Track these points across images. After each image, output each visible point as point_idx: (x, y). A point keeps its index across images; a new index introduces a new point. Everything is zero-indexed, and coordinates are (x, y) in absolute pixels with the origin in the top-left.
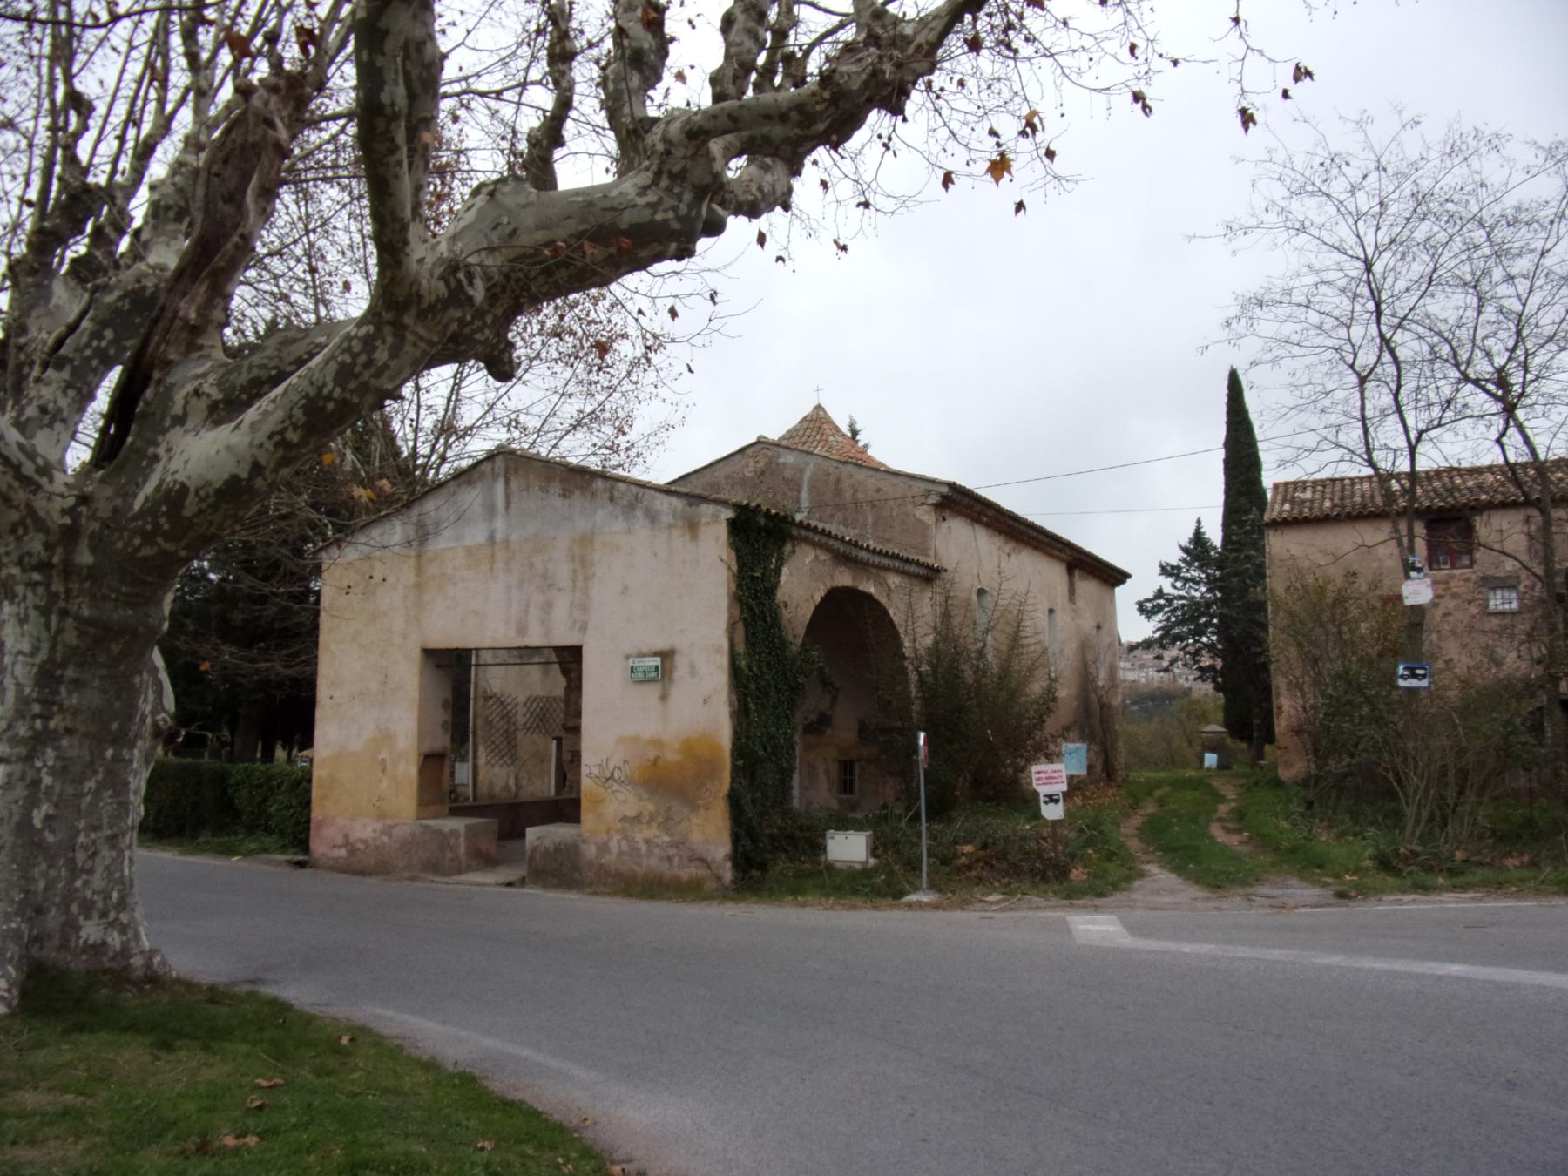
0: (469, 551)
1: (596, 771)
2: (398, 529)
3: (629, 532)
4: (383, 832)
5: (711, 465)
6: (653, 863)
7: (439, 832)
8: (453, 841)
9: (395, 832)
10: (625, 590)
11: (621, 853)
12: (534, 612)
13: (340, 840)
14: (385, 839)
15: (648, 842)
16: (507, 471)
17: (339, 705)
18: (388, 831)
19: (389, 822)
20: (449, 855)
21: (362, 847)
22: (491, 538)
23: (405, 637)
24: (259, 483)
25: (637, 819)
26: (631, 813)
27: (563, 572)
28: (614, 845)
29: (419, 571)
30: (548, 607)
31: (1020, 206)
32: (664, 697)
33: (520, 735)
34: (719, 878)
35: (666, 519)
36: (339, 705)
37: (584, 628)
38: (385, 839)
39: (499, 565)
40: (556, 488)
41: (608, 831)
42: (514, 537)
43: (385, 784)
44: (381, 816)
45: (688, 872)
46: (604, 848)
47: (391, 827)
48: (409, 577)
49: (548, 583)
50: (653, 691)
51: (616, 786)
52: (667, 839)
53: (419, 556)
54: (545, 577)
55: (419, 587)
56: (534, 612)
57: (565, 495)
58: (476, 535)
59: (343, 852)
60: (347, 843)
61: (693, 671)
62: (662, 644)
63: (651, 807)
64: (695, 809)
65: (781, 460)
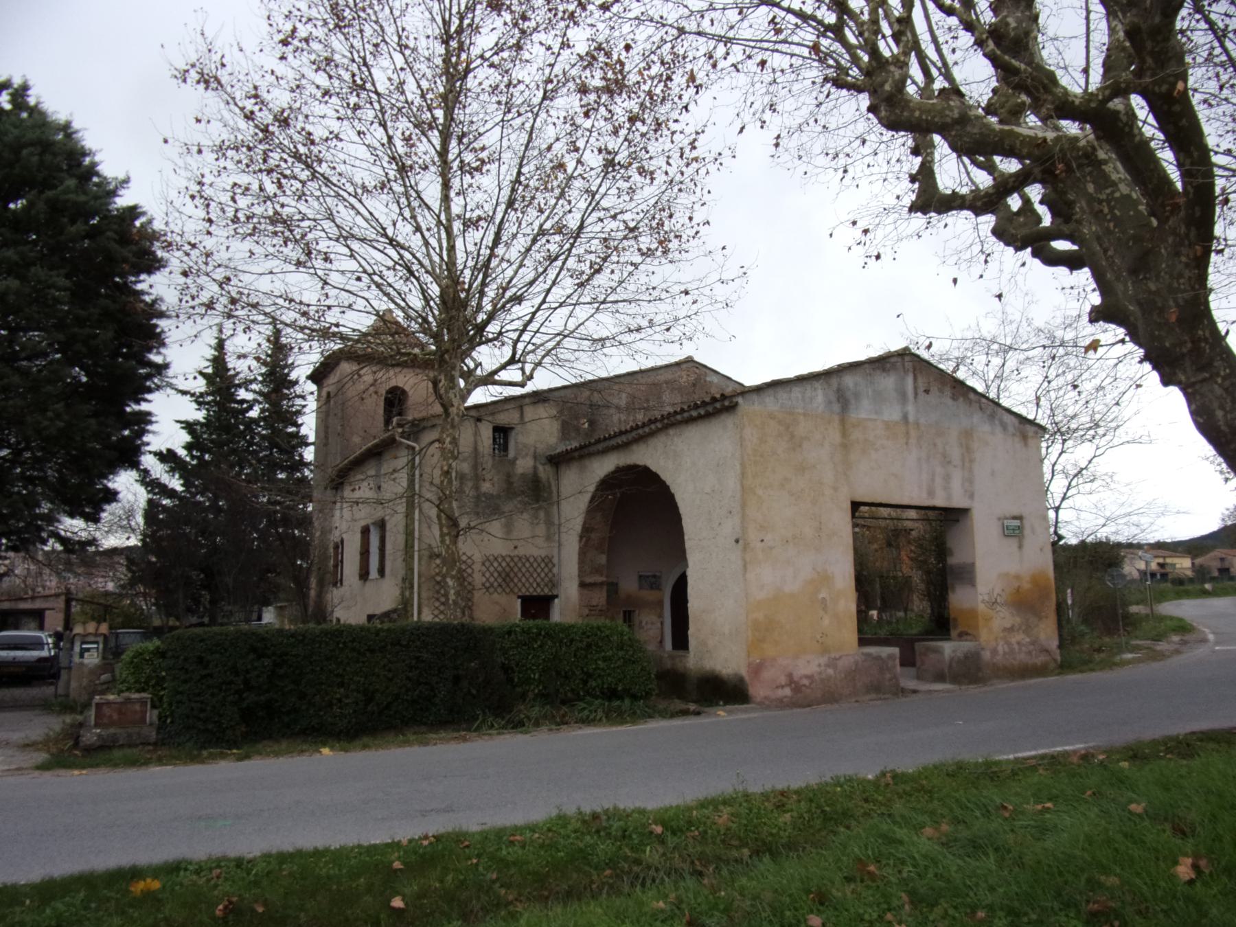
0: (888, 425)
1: (986, 598)
2: (820, 392)
3: (993, 433)
4: (828, 666)
5: (801, 380)
6: (1022, 657)
7: (878, 658)
8: (890, 663)
9: (840, 663)
10: (993, 474)
11: (1005, 653)
12: (939, 481)
13: (783, 680)
14: (830, 671)
15: (1018, 643)
16: (914, 370)
17: (771, 548)
18: (832, 663)
19: (833, 655)
20: (888, 676)
21: (806, 682)
22: (905, 417)
23: (835, 489)
24: (319, 263)
25: (1011, 630)
26: (1008, 626)
27: (955, 453)
28: (1000, 649)
29: (844, 434)
30: (947, 478)
31: (955, 281)
32: (1020, 547)
33: (477, 595)
34: (1055, 661)
35: (1011, 429)
36: (771, 548)
37: (972, 496)
38: (830, 671)
39: (913, 441)
40: (948, 392)
41: (996, 639)
42: (922, 421)
43: (826, 621)
44: (825, 650)
45: (1040, 659)
46: (994, 652)
47: (836, 659)
48: (834, 435)
49: (946, 461)
50: (1013, 543)
51: (999, 608)
52: (1028, 640)
53: (843, 421)
54: (944, 456)
55: (845, 446)
56: (939, 481)
57: (954, 398)
58: (892, 413)
59: (787, 692)
60: (791, 682)
61: (1033, 532)
62: (1016, 512)
63: (1018, 620)
64: (1040, 619)
65: (708, 379)
